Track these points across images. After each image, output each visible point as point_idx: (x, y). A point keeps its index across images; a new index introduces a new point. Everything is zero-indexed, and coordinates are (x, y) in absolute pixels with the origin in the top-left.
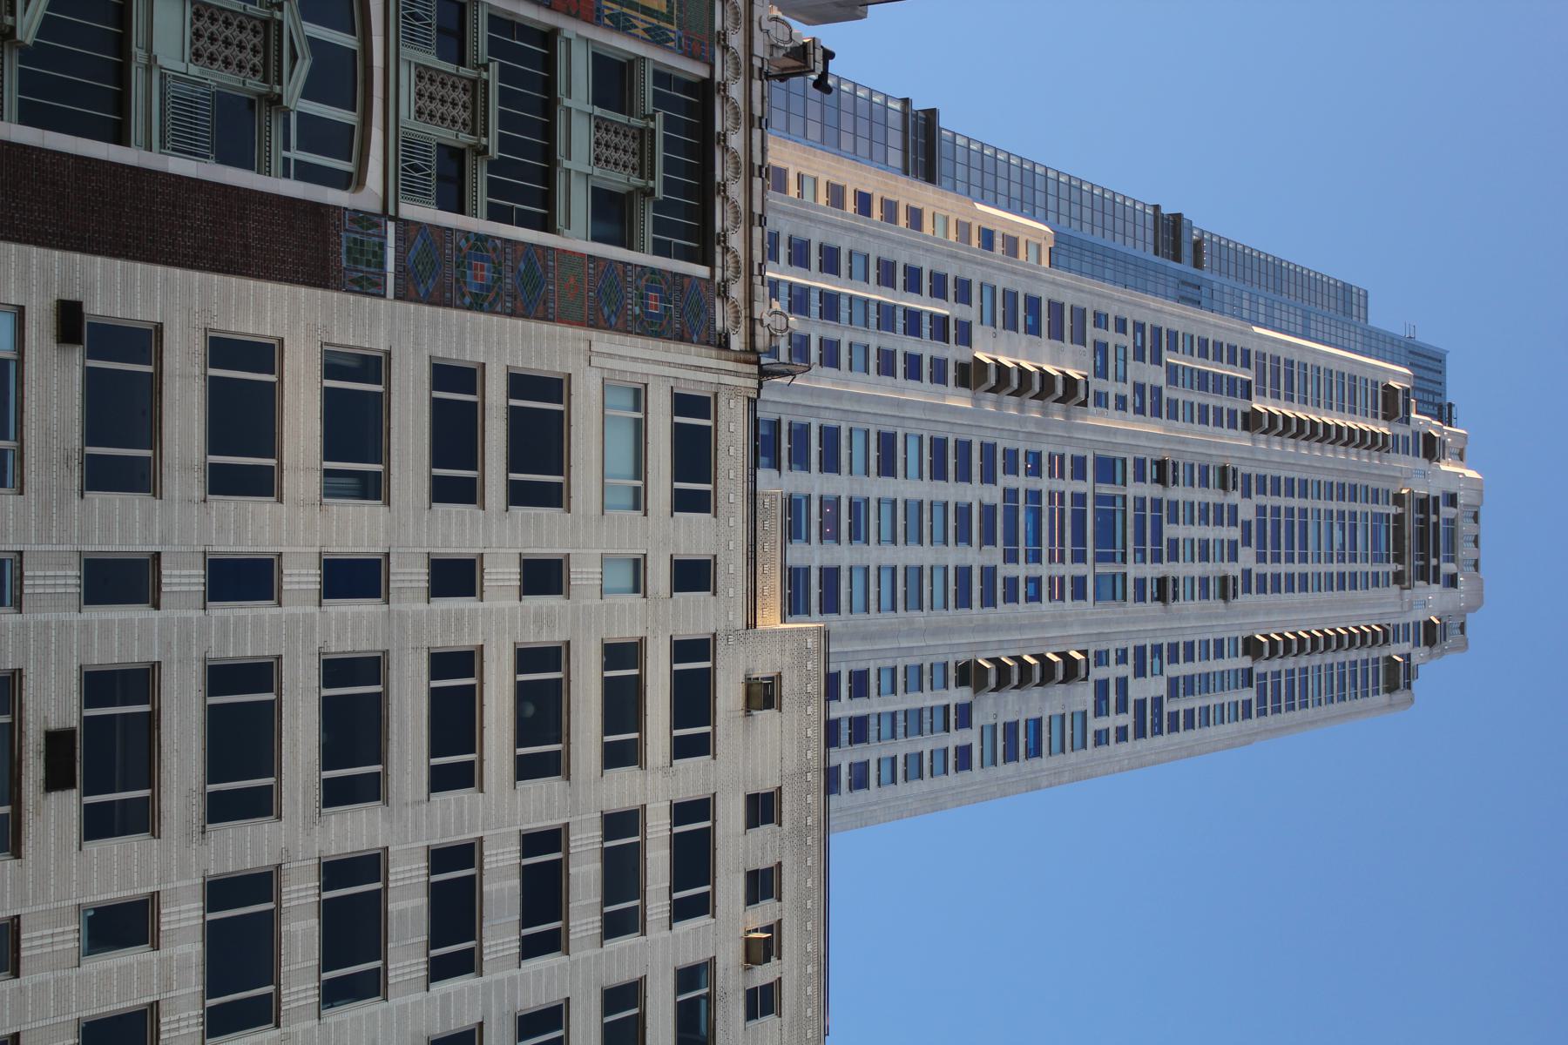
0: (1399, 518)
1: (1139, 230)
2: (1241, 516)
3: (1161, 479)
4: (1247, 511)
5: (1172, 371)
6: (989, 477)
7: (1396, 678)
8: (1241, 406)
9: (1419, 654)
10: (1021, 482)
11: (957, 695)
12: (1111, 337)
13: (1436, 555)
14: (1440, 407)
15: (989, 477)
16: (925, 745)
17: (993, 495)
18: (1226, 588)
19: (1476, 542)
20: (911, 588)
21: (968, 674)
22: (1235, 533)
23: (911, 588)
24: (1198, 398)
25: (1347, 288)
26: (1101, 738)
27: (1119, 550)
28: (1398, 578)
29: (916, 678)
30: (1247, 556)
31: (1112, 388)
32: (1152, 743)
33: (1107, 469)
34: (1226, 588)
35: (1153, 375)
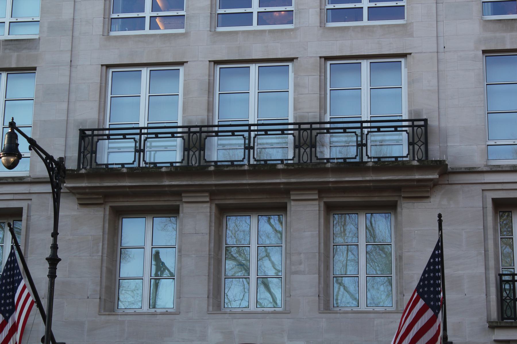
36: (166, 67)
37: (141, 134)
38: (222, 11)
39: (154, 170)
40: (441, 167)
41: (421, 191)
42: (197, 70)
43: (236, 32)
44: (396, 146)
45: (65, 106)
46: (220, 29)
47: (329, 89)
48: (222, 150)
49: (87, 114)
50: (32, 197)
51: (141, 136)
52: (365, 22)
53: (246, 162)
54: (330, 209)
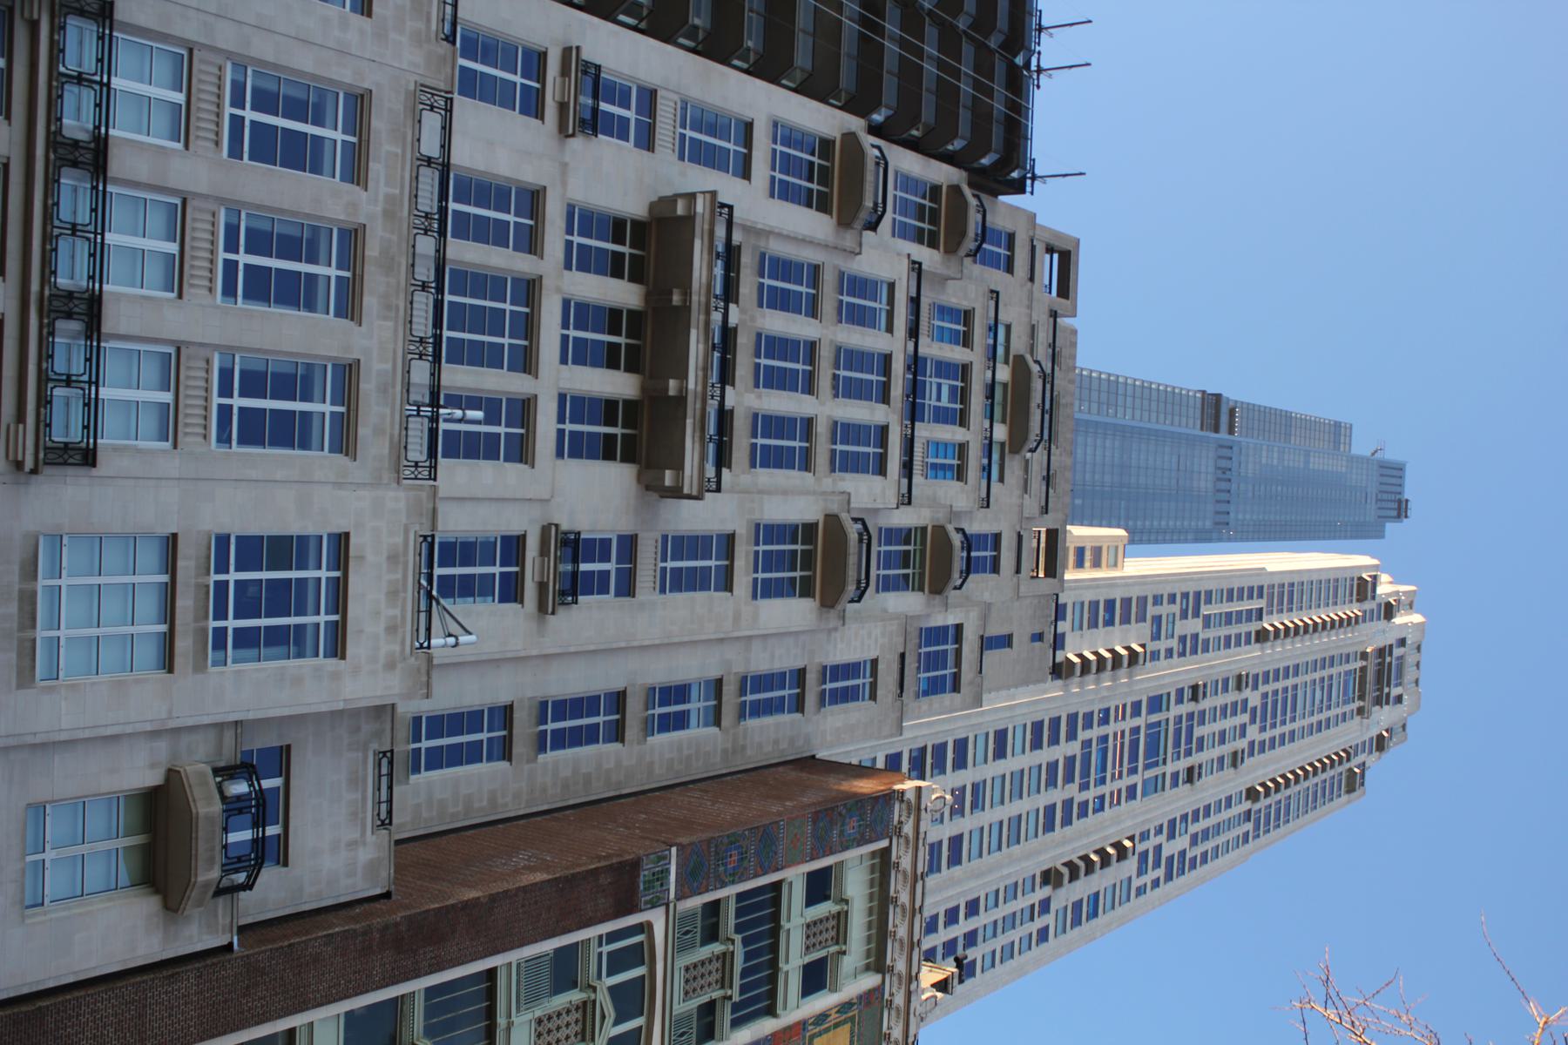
0: (1363, 669)
1: (1191, 411)
2: (1250, 705)
3: (1194, 698)
4: (1254, 699)
5: (1207, 619)
6: (1072, 736)
7: (1353, 783)
8: (1253, 627)
9: (1372, 760)
10: (1095, 732)
11: (1043, 893)
12: (1165, 610)
13: (1389, 685)
14: (1400, 502)
15: (1072, 736)
16: (1014, 935)
17: (1074, 748)
18: (1236, 759)
19: (1418, 665)
20: (1013, 831)
21: (1050, 877)
22: (1245, 718)
23: (1013, 831)
24: (1224, 631)
25: (1337, 425)
26: (1141, 891)
27: (1161, 757)
28: (1360, 711)
29: (1013, 891)
30: (1253, 733)
31: (1162, 645)
32: (1178, 882)
33: (1156, 703)
34: (1236, 759)
35: (1193, 626)
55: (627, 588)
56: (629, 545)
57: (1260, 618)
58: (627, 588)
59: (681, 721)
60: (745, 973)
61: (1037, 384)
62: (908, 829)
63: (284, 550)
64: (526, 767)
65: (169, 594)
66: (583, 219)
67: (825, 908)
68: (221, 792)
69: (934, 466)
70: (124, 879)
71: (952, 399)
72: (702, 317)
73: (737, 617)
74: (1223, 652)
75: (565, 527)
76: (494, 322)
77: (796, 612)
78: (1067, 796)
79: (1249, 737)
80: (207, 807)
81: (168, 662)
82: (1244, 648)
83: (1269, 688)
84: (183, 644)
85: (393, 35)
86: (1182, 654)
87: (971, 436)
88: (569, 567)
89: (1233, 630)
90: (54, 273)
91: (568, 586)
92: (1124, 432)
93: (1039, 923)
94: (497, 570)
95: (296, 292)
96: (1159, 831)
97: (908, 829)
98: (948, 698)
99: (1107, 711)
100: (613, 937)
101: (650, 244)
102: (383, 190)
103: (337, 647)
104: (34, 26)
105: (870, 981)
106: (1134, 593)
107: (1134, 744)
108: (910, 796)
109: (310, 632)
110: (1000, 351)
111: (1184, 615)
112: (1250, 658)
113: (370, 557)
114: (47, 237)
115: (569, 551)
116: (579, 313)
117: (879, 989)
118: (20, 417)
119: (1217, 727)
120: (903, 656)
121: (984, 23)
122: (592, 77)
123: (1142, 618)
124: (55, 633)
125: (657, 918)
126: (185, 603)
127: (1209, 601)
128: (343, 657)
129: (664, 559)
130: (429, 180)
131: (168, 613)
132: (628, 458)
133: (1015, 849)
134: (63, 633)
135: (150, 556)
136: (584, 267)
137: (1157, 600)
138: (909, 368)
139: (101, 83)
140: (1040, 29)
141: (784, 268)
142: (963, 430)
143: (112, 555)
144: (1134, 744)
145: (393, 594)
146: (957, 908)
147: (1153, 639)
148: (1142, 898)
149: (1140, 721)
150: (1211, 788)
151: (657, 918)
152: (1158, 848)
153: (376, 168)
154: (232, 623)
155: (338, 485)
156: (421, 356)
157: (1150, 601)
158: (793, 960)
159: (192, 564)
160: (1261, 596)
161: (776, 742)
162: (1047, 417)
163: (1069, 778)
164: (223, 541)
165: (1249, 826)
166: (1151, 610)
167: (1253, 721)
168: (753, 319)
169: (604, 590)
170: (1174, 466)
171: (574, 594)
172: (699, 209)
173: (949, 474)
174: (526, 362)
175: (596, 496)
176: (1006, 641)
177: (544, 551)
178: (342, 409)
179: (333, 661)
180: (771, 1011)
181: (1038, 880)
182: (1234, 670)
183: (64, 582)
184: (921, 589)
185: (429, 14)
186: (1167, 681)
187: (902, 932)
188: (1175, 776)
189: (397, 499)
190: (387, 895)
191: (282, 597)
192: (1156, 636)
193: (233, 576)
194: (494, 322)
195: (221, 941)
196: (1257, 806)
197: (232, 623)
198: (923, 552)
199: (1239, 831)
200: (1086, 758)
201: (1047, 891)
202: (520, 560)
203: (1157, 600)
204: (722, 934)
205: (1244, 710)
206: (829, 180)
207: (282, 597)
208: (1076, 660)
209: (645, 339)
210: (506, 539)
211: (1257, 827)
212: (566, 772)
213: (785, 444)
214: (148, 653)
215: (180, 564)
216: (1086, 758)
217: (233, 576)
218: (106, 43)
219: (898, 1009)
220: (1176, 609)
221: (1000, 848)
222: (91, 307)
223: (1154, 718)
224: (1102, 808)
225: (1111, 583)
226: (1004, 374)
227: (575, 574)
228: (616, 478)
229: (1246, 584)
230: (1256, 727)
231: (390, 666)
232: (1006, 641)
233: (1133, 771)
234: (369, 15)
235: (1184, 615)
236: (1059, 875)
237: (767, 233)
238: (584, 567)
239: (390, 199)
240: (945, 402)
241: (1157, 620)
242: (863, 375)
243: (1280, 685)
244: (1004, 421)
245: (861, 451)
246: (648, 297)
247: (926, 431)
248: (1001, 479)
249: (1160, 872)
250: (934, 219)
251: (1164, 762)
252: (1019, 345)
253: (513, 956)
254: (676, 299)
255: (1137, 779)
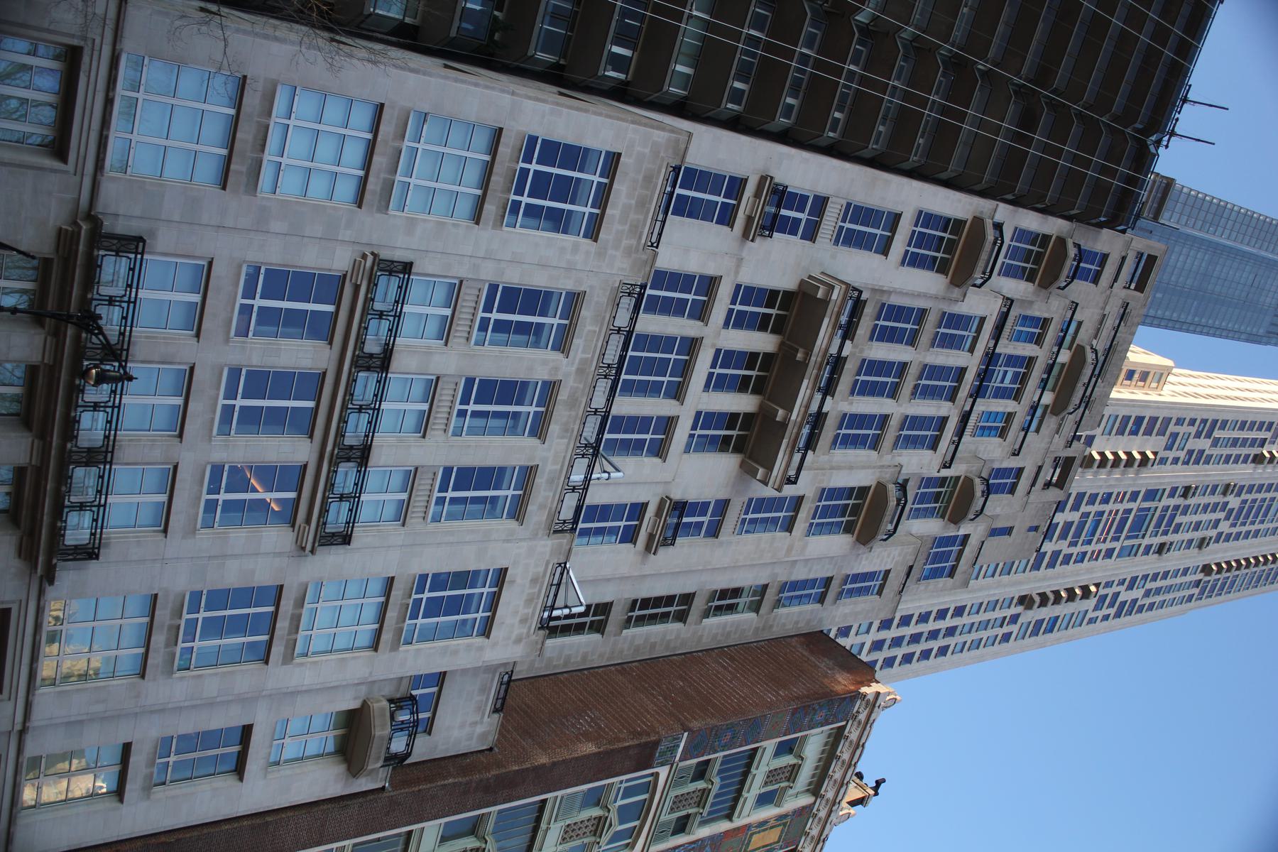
3: (1185, 496)
6: (1076, 507)
8: (1255, 451)
16: (983, 634)
17: (1075, 517)
18: (1202, 543)
21: (1025, 601)
22: (1222, 515)
29: (993, 605)
31: (1171, 455)
32: (1123, 620)
33: (1151, 495)
35: (1204, 444)
36: (196, 321)
37: (129, 302)
38: (263, 271)
39: (59, 511)
40: (49, 577)
41: (27, 552)
42: (185, 348)
43: (218, 389)
44: (78, 529)
45: (177, 218)
46: (244, 269)
47: (179, 260)
48: (85, 478)
49: (164, 240)
50: (78, 178)
51: (99, 508)
52: (222, 401)
53: (96, 296)
54: (47, 262)
55: (811, 234)
56: (723, 506)
57: (1262, 445)
58: (811, 234)
59: (731, 608)
60: (713, 805)
61: (1088, 371)
62: (862, 717)
63: (463, 578)
64: (613, 639)
65: (384, 608)
66: (746, 294)
67: (788, 760)
68: (392, 718)
69: (983, 428)
70: (331, 747)
71: (1013, 381)
72: (815, 371)
73: (790, 550)
74: (1221, 466)
75: (777, 180)
76: (661, 367)
77: (838, 543)
78: (1057, 548)
79: (1220, 529)
80: (381, 730)
81: (477, 217)
82: (1240, 465)
83: (1250, 497)
84: (386, 637)
85: (610, 252)
86: (1186, 463)
87: (1019, 409)
88: (773, 210)
89: (1235, 451)
90: (373, 300)
91: (768, 224)
92: (1217, 249)
93: (1006, 629)
94: (720, 199)
95: (532, 334)
96: (1122, 583)
97: (862, 717)
98: (943, 582)
99: (1110, 495)
100: (627, 781)
101: (792, 311)
102: (580, 355)
103: (593, 232)
104: (357, 288)
105: (806, 800)
106: (1162, 415)
107: (1123, 521)
108: (871, 698)
109: (523, 418)
110: (1068, 338)
111: (1198, 435)
112: (1243, 473)
113: (519, 581)
114: (344, 407)
115: (776, 198)
116: (726, 357)
117: (811, 806)
118: (308, 521)
119: (1195, 518)
120: (911, 567)
121: (1127, 117)
122: (781, 195)
123: (1162, 433)
124: (408, 180)
125: (663, 772)
126: (497, 180)
127: (1223, 427)
128: (488, 637)
129: (844, 221)
130: (616, 341)
131: (485, 183)
132: (737, 450)
133: (1005, 578)
134: (413, 181)
135: (481, 140)
136: (738, 325)
137: (1180, 422)
138: (979, 375)
139: (374, 409)
140: (1185, 100)
141: (898, 313)
142: (1015, 403)
143: (456, 135)
144: (1123, 521)
145: (529, 601)
146: (947, 610)
147: (1166, 449)
148: (1091, 626)
149: (1134, 506)
150: (1173, 561)
151: (663, 772)
152: (1117, 595)
153: (578, 343)
154: (525, 199)
155: (508, 541)
156: (629, 294)
157: (1173, 421)
158: (755, 787)
159: (401, 593)
160: (1269, 429)
161: (797, 623)
162: (1094, 380)
163: (1063, 536)
164: (533, 140)
165: (1196, 591)
166: (1172, 428)
167: (1227, 518)
168: (862, 351)
169: (793, 232)
170: (1249, 282)
171: (771, 230)
172: (834, 297)
173: (993, 432)
174: (677, 392)
175: (705, 475)
176: (1008, 531)
177: (757, 195)
178: (605, 181)
179: (588, 241)
180: (729, 817)
181: (1015, 601)
182: (1226, 480)
183: (421, 146)
184: (943, 517)
185: (641, 233)
186: (1167, 480)
187: (838, 776)
188: (1148, 547)
189: (547, 547)
190: (491, 749)
191: (565, 189)
192: (1169, 447)
193: (534, 167)
194: (661, 367)
195: (380, 785)
196: (1208, 578)
197: (525, 199)
198: (952, 493)
199: (1187, 593)
200: (1082, 525)
201: (1020, 609)
202: (739, 198)
203: (1180, 422)
204: (707, 776)
205: (1223, 510)
206: (952, 251)
207: (565, 189)
208: (1097, 457)
209: (770, 377)
210: (733, 179)
211: (1202, 593)
212: (639, 641)
213: (863, 432)
214: (465, 207)
215: (393, 593)
216: (1082, 525)
217: (534, 167)
218: (403, 289)
219: (859, 722)
220: (1193, 430)
221: (993, 576)
222: (363, 453)
223: (1146, 505)
224: (1082, 561)
225: (1145, 405)
226: (1065, 356)
227: (776, 216)
228: (726, 463)
229: (1259, 419)
230: (1228, 523)
231: (518, 640)
232: (1008, 531)
233: (1116, 539)
234: (596, 241)
235: (1198, 435)
236: (1032, 601)
237: (889, 293)
238: (784, 212)
239: (584, 362)
240: (1007, 383)
241: (1174, 436)
242: (940, 382)
243: (1259, 496)
244: (1053, 390)
245: (923, 433)
246: (782, 345)
247: (982, 405)
248: (1037, 431)
249: (1112, 611)
250: (1039, 256)
251: (1143, 537)
252: (1083, 337)
253: (559, 793)
254: (800, 356)
255: (1117, 545)
